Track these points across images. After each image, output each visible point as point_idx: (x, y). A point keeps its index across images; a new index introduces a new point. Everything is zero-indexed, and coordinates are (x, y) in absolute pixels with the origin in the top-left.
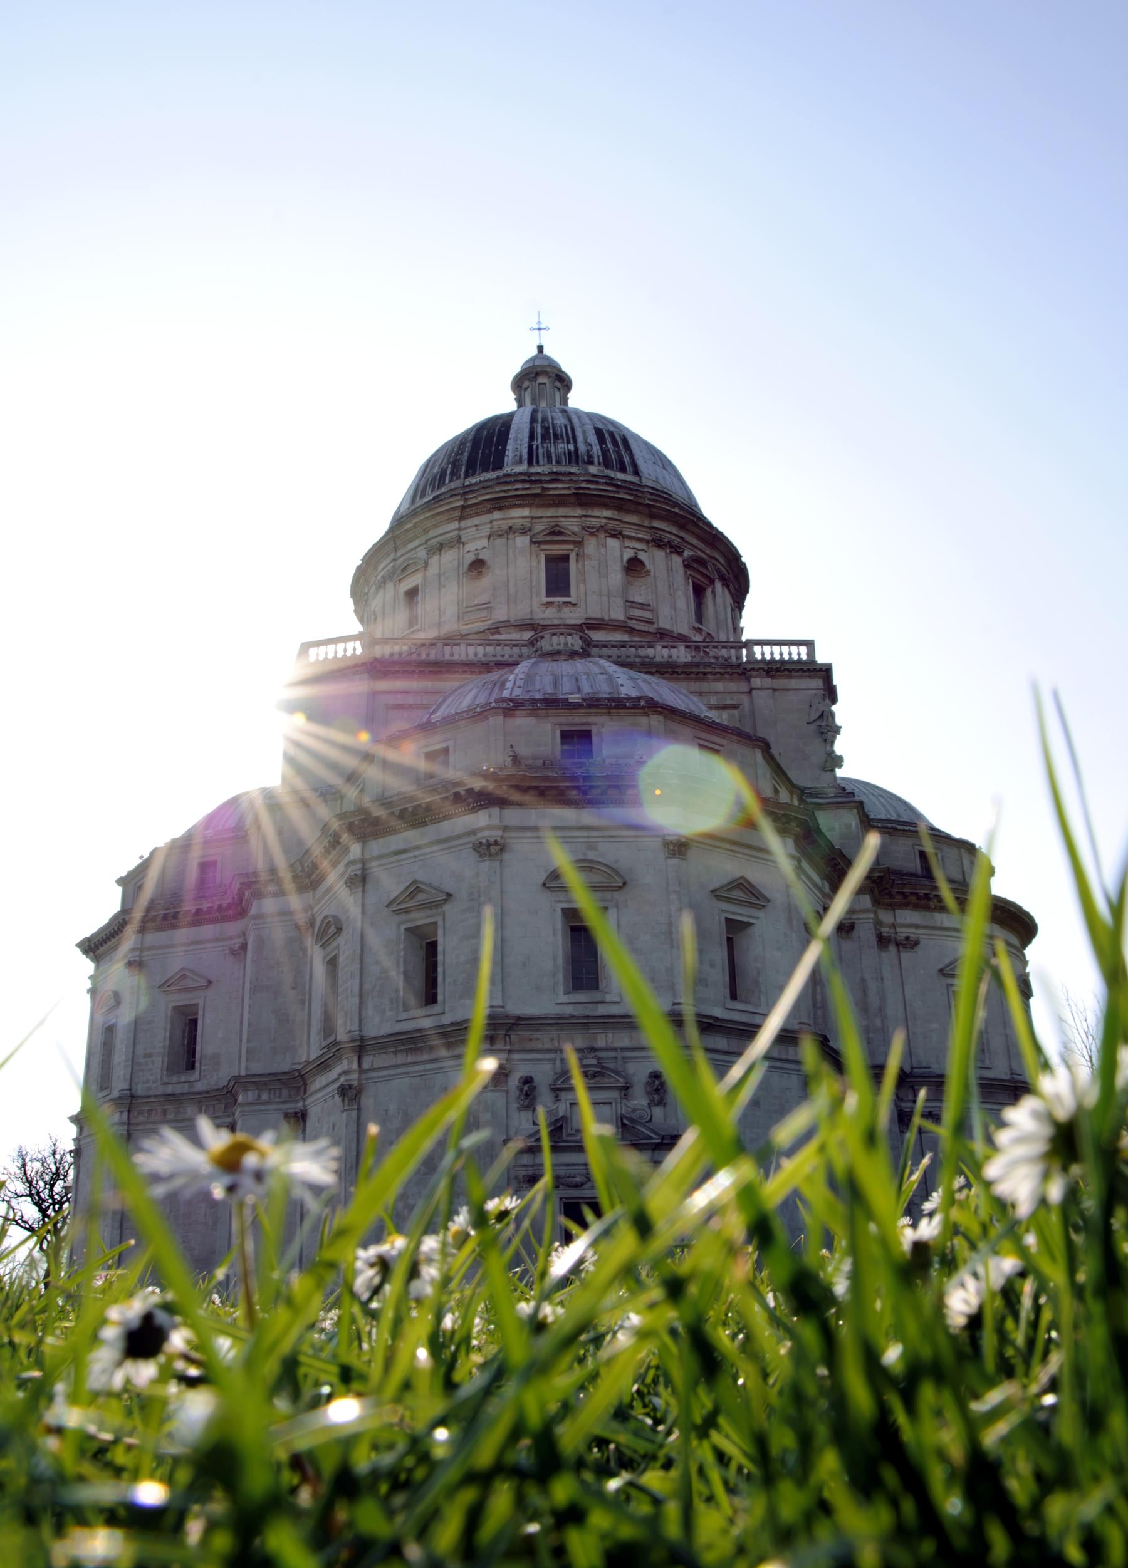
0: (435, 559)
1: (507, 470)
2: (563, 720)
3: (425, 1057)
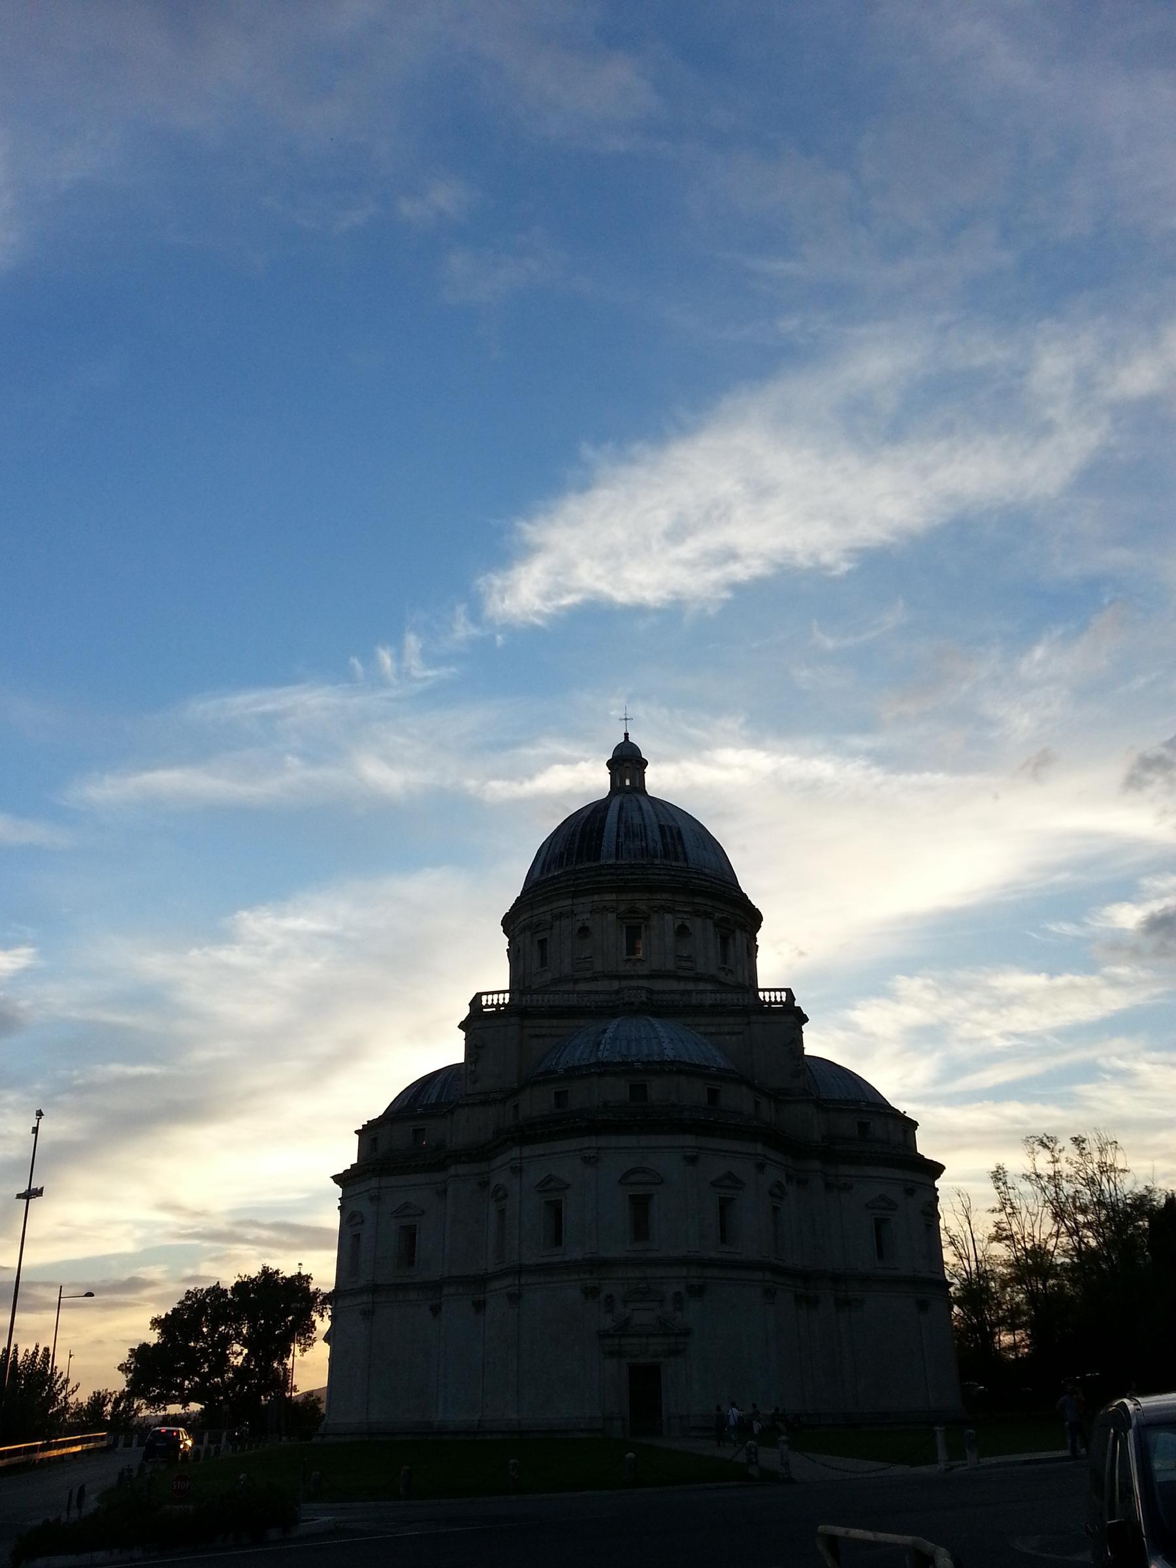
1: (602, 862)
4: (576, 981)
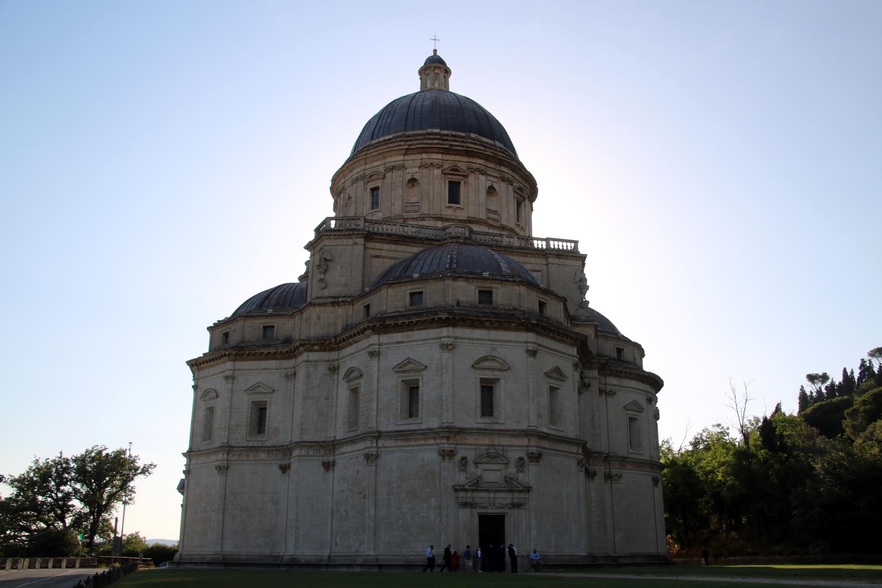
0: (389, 175)
2: (480, 284)
3: (412, 443)
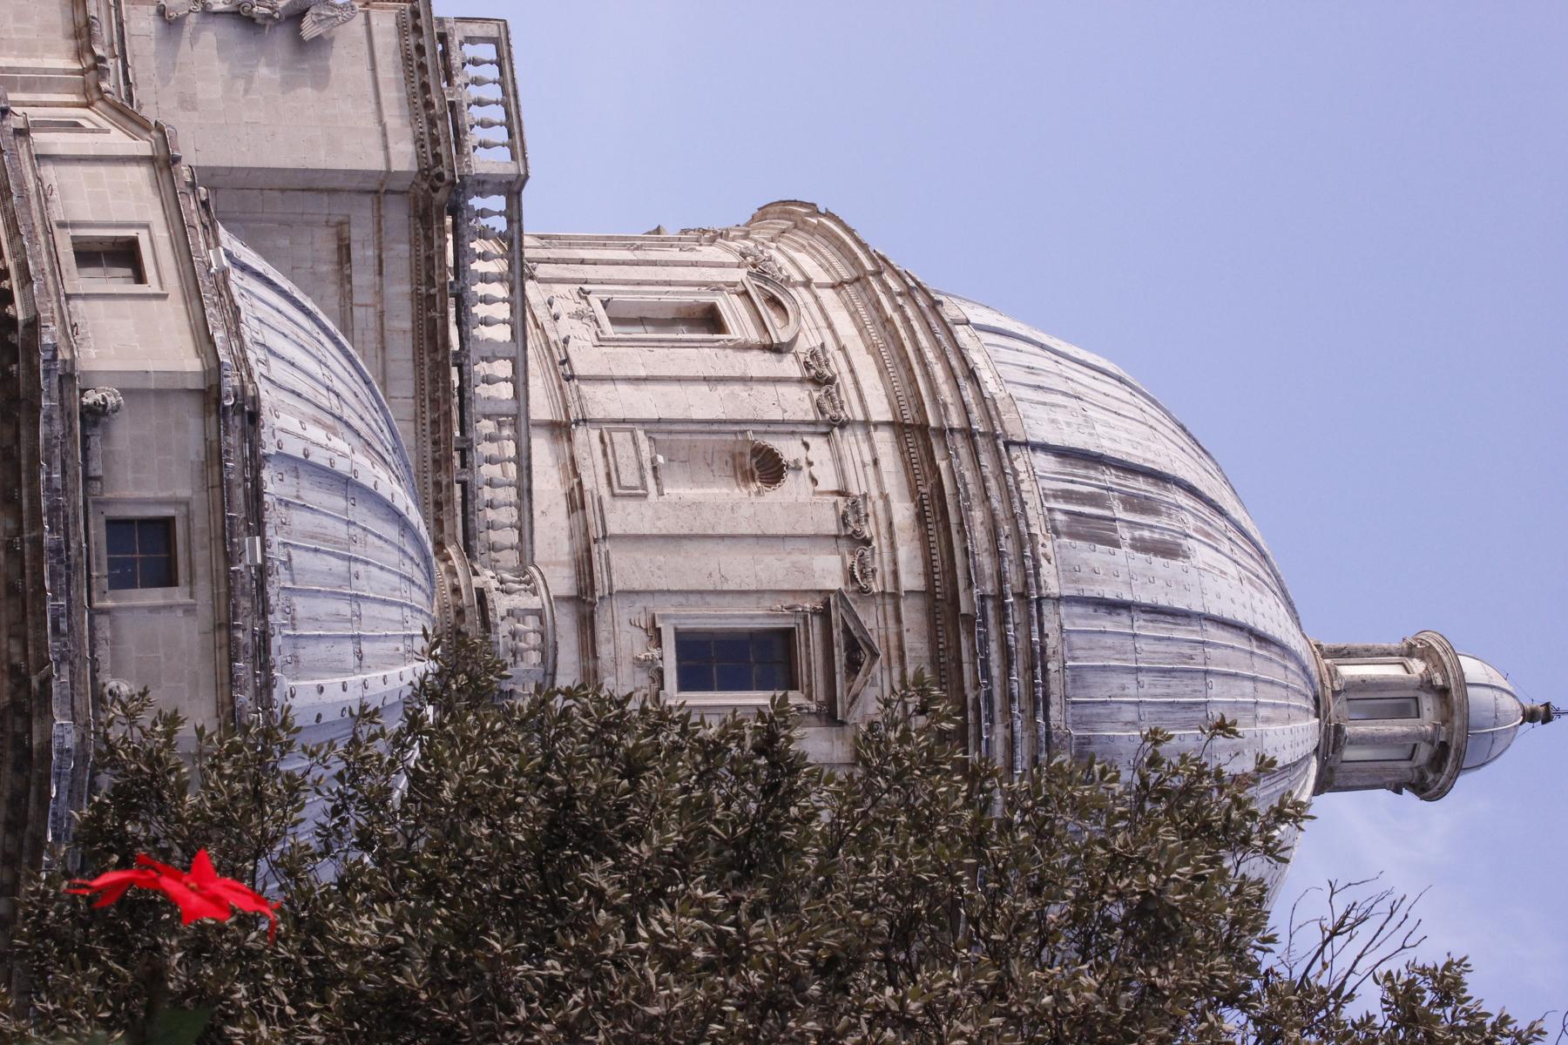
0: (789, 366)
1: (1047, 546)
2: (199, 523)
4: (561, 430)
